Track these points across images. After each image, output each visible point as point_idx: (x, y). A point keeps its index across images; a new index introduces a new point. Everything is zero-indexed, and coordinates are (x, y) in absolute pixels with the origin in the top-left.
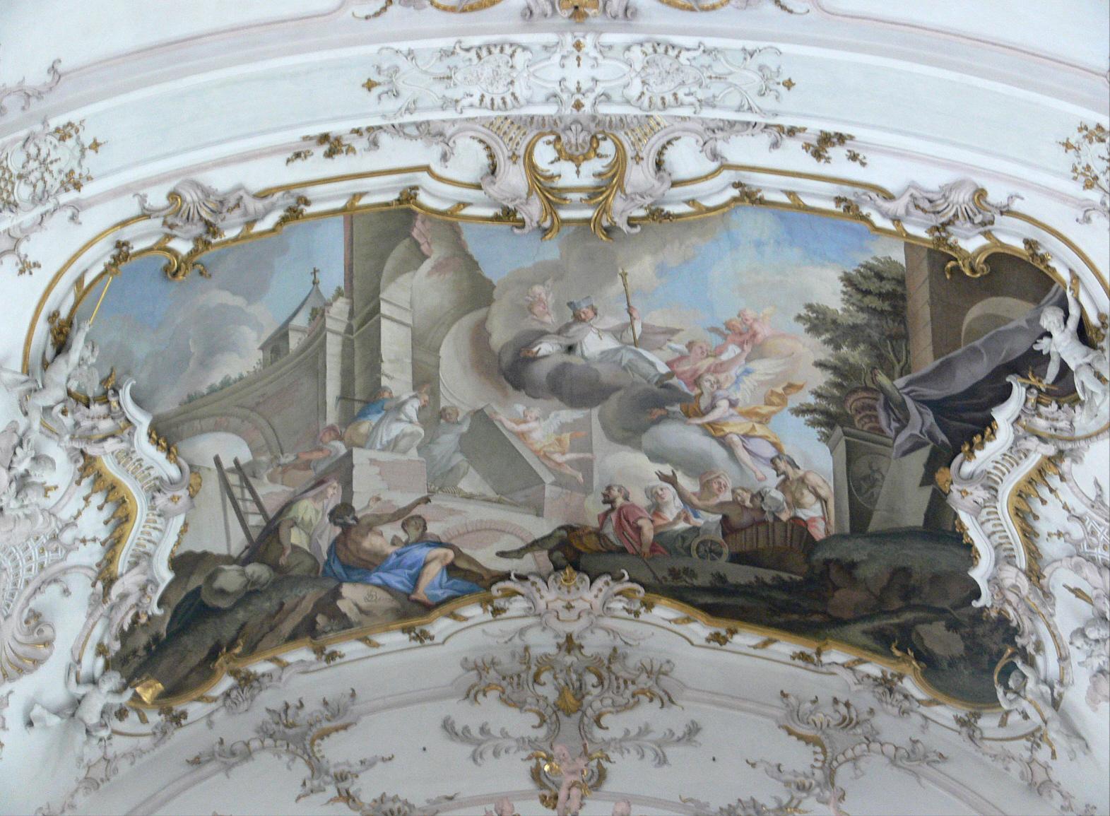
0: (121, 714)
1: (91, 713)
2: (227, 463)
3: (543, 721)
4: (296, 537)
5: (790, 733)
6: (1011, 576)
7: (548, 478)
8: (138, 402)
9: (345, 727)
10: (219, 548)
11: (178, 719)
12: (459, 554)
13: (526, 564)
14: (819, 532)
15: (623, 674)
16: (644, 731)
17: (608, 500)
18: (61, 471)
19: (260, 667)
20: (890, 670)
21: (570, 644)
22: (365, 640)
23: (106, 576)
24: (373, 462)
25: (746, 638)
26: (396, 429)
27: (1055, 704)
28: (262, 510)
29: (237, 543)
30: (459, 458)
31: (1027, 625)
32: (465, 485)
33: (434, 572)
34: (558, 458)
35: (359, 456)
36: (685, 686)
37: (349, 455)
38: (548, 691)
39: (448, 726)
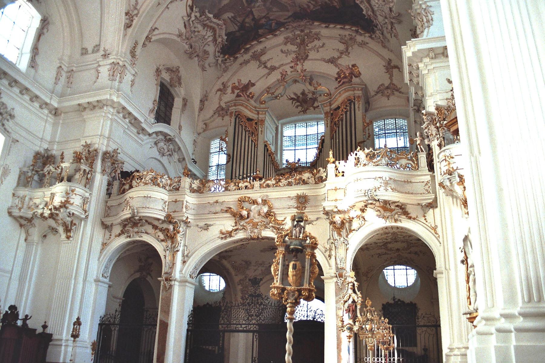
0: (226, 60)
1: (220, 62)
2: (230, 17)
3: (298, 47)
4: (247, 25)
5: (341, 42)
6: (370, 13)
7: (288, 6)
8: (209, 12)
9: (264, 54)
10: (234, 30)
11: (237, 58)
12: (277, 21)
13: (290, 20)
14: (338, 7)
15: (311, 35)
16: (316, 46)
17: (300, 7)
18: (200, 27)
19: (248, 46)
20: (357, 29)
21: (302, 31)
22: (265, 38)
23: (215, 40)
24: (256, 10)
25: (332, 26)
26: (258, 4)
27: (382, 34)
28: (239, 22)
29: (237, 28)
30: (271, 6)
31: (375, 21)
32: (274, 10)
33: (274, 24)
34: (289, 2)
35: (253, 9)
36: (322, 36)
37: (251, 10)
38: (299, 41)
39: (282, 51)
